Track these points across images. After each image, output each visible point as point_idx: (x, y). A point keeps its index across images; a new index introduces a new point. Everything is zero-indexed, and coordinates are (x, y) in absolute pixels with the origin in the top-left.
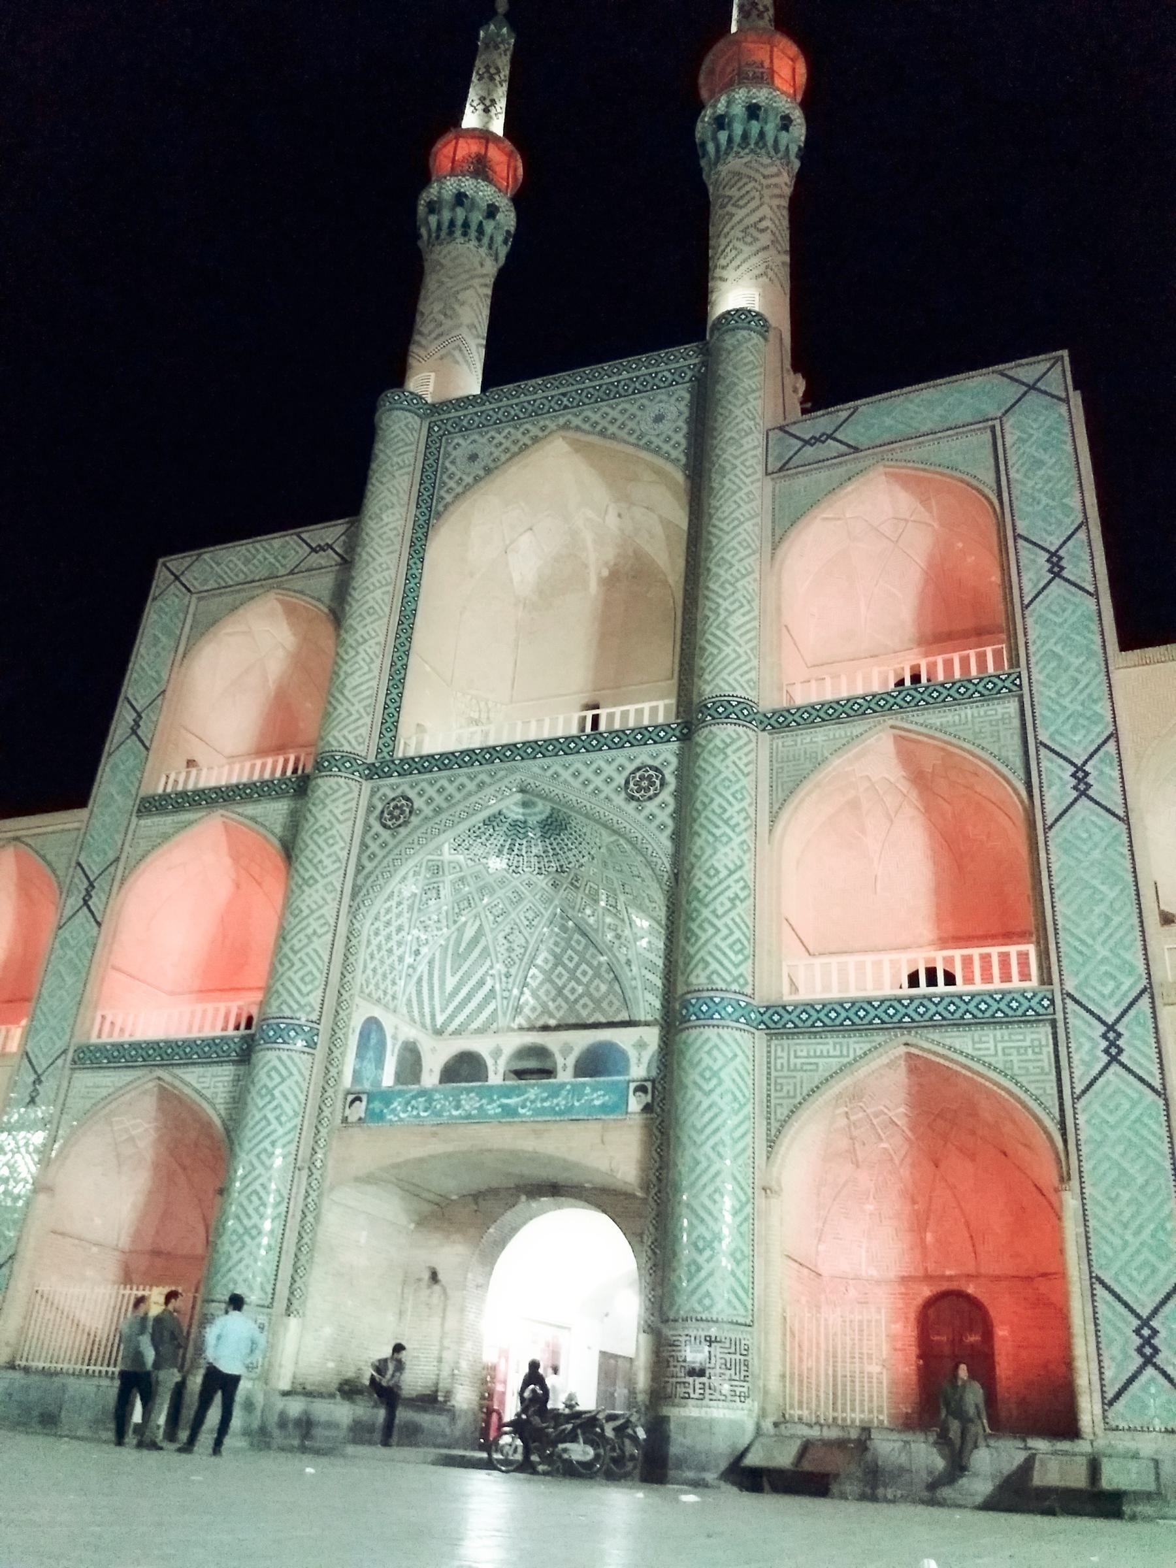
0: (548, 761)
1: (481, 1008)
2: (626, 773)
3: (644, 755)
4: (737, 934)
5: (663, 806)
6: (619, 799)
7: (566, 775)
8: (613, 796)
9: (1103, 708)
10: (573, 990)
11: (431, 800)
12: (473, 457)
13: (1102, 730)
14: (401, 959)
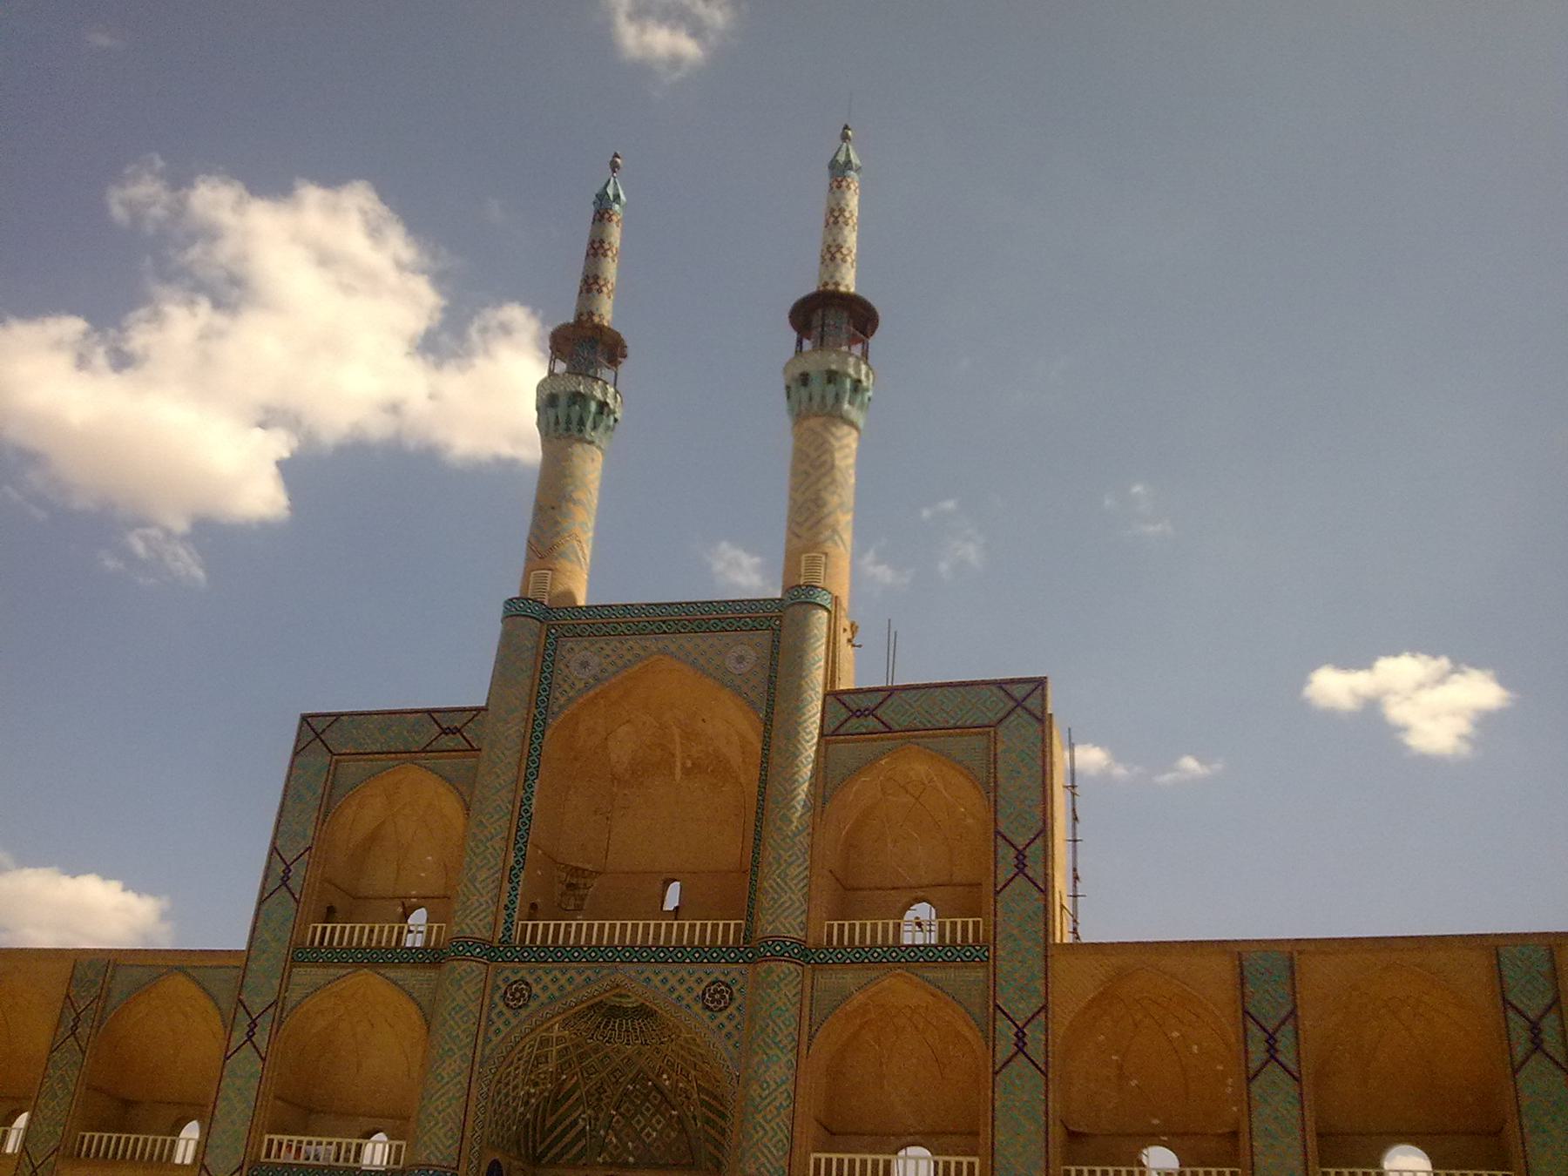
0: (641, 967)
1: (573, 1143)
2: (703, 985)
3: (717, 972)
4: (780, 1136)
5: (730, 1017)
6: (697, 1008)
7: (656, 981)
8: (692, 1004)
9: (1039, 985)
10: (649, 1135)
11: (545, 988)
12: (585, 665)
13: (1036, 1003)
14: (515, 1110)
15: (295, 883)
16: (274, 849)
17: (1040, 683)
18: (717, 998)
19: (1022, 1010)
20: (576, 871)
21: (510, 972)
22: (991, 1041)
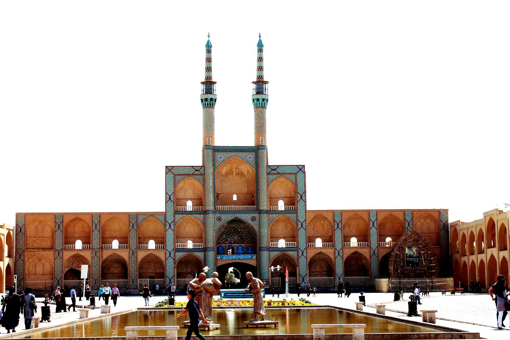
3: (253, 215)
12: (221, 158)
15: (172, 199)
16: (166, 193)
17: (304, 166)
18: (253, 219)
19: (302, 220)
20: (218, 194)
21: (218, 215)
22: (297, 225)
